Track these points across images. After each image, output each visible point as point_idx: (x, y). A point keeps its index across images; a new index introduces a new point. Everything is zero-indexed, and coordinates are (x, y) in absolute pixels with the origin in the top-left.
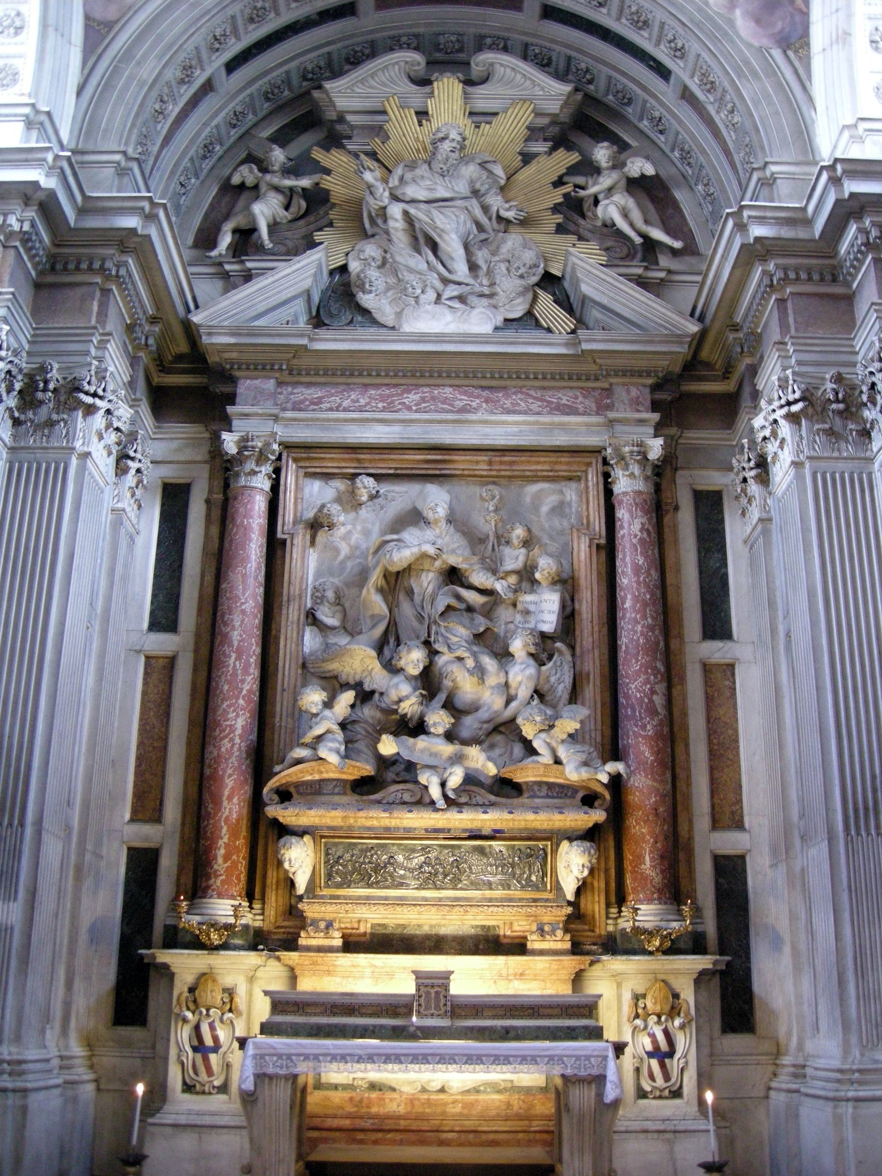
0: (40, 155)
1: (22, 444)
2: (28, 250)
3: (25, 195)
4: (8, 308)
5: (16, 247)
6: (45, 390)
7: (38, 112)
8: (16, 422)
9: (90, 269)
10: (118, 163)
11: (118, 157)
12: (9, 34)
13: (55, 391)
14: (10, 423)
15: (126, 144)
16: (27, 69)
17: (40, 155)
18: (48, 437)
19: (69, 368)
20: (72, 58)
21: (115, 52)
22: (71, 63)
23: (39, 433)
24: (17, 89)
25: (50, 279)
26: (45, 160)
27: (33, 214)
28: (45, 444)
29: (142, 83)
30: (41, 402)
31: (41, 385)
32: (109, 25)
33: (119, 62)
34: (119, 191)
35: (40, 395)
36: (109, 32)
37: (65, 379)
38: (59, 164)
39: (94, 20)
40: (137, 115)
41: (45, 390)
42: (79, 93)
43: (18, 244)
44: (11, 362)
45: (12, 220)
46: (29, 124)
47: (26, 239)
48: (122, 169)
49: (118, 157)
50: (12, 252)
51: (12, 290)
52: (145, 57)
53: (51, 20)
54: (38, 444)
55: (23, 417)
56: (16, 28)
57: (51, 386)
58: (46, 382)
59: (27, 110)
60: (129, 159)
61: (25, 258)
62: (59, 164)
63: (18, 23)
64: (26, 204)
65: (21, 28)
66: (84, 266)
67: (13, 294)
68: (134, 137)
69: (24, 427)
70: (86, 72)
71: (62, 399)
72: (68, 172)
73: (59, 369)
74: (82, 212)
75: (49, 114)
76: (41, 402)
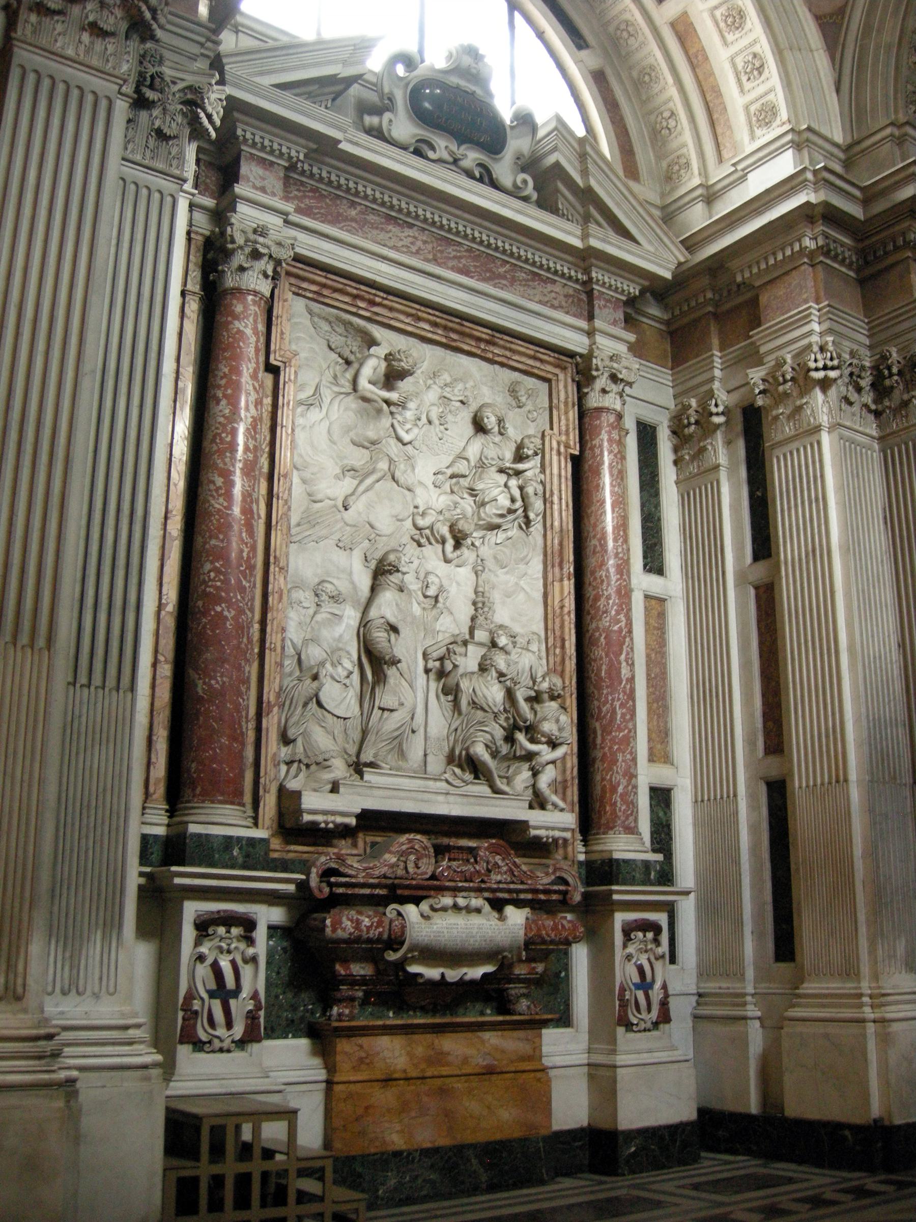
0: (801, 179)
1: (888, 431)
2: (835, 258)
3: (807, 216)
4: (831, 319)
5: (821, 262)
6: (891, 375)
7: (800, 133)
8: (877, 414)
9: (897, 248)
10: (892, 135)
11: (888, 131)
12: (754, 78)
13: (900, 373)
14: (871, 417)
15: (896, 112)
16: (780, 99)
17: (801, 179)
18: (907, 416)
19: (905, 347)
20: (818, 62)
21: (855, 33)
22: (820, 67)
23: (898, 416)
24: (778, 122)
25: (868, 271)
26: (806, 180)
27: (822, 228)
28: (906, 425)
29: (889, 47)
30: (892, 388)
31: (886, 372)
32: (841, 11)
33: (862, 40)
34: (903, 160)
35: (887, 382)
36: (843, 18)
37: (905, 358)
38: (819, 176)
39: (825, 16)
40: (896, 80)
41: (891, 375)
42: (838, 91)
43: (821, 258)
44: (851, 364)
45: (808, 243)
46: (798, 146)
47: (825, 251)
48: (898, 138)
49: (888, 131)
50: (819, 267)
51: (826, 303)
52: (882, 22)
53: (784, 43)
54: (901, 427)
55: (880, 407)
56: (757, 69)
57: (895, 370)
58: (889, 368)
59: (789, 137)
60: (900, 126)
61: (836, 265)
62: (819, 176)
63: (757, 65)
64: (812, 223)
65: (762, 66)
66: (891, 247)
67: (829, 305)
68: (901, 103)
69: (884, 415)
70: (837, 66)
71: (908, 377)
72: (832, 178)
73: (897, 352)
74: (866, 202)
75: (809, 129)
76: (892, 388)
